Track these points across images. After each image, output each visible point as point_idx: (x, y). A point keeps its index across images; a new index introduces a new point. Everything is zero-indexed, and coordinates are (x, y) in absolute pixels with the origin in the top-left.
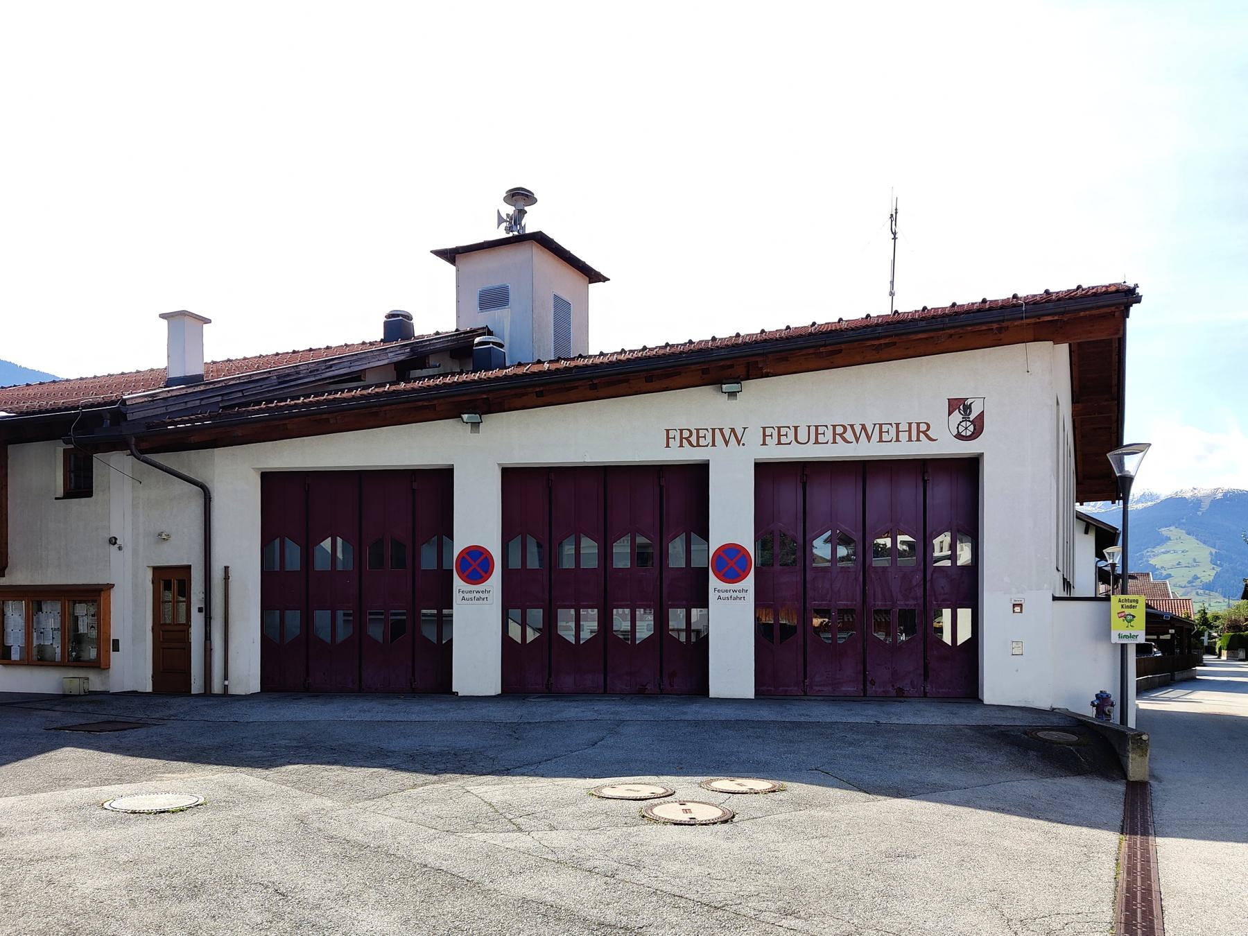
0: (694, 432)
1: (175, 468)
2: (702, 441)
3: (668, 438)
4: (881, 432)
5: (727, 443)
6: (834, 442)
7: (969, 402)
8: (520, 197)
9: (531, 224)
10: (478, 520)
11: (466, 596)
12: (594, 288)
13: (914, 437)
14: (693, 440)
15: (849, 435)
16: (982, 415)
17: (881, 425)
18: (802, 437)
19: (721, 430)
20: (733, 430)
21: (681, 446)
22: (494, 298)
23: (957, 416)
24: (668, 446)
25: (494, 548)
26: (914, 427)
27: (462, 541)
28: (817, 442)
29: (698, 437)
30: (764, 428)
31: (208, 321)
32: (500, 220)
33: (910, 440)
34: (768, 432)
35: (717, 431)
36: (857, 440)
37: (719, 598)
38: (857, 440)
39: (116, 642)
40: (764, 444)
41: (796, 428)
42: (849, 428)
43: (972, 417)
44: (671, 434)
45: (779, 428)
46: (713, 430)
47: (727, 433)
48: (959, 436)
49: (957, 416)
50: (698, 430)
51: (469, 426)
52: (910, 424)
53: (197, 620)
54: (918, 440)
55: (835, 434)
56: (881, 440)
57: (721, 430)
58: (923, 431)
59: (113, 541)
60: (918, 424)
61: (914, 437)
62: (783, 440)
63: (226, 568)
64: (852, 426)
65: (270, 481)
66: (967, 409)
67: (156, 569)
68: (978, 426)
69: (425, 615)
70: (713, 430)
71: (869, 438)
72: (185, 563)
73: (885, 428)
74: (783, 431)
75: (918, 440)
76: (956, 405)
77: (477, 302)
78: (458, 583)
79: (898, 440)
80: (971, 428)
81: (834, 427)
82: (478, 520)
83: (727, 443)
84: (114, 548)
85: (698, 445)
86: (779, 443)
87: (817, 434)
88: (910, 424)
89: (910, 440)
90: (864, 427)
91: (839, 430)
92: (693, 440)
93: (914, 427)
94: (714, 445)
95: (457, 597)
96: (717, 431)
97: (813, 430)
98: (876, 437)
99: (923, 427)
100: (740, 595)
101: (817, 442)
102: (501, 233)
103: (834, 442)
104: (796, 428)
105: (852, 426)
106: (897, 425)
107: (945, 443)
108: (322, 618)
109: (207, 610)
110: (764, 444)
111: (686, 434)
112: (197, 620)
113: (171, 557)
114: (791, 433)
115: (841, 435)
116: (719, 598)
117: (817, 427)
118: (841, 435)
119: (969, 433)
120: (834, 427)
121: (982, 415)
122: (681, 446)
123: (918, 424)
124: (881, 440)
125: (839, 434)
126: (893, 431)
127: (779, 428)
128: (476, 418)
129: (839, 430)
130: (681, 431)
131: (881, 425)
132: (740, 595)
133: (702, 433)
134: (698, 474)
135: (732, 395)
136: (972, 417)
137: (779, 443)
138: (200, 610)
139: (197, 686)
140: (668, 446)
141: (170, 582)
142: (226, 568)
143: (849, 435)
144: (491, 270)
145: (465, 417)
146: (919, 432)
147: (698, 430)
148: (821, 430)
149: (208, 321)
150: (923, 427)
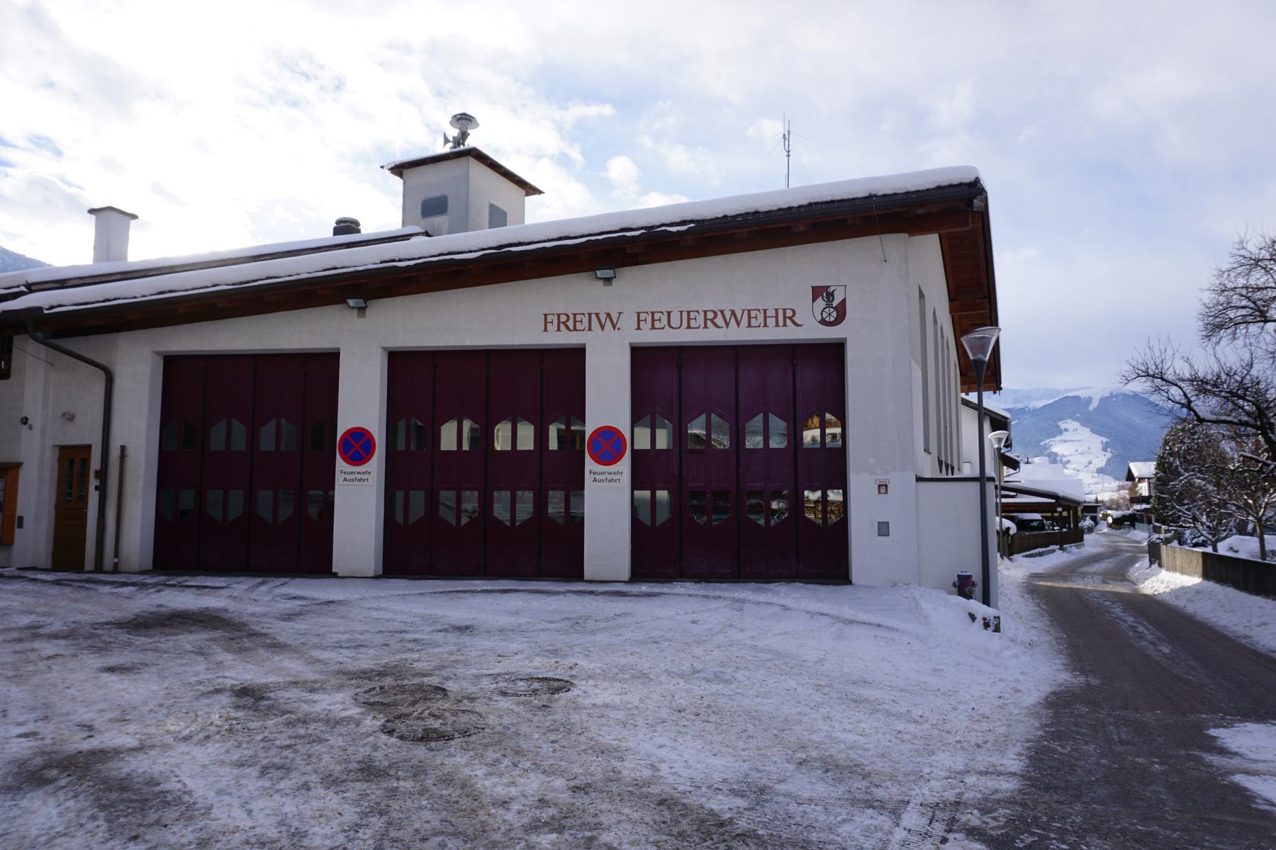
1: (77, 351)
2: (579, 326)
3: (546, 323)
4: (749, 318)
5: (603, 327)
6: (706, 327)
7: (831, 289)
8: (464, 120)
9: (470, 143)
10: (361, 402)
11: (349, 477)
12: (531, 200)
13: (781, 323)
14: (571, 324)
15: (719, 321)
16: (843, 302)
17: (749, 311)
18: (675, 321)
19: (597, 315)
20: (608, 315)
21: (559, 330)
22: (433, 207)
23: (821, 303)
24: (546, 330)
25: (377, 429)
26: (781, 312)
27: (346, 421)
28: (689, 327)
29: (575, 322)
30: (639, 314)
31: (134, 217)
32: (446, 141)
33: (777, 325)
34: (642, 317)
35: (594, 317)
36: (727, 324)
37: (595, 480)
38: (727, 324)
39: (21, 518)
40: (639, 328)
41: (669, 313)
43: (835, 304)
44: (549, 318)
45: (653, 313)
46: (590, 315)
47: (603, 317)
48: (823, 322)
49: (821, 303)
50: (575, 315)
51: (355, 312)
52: (777, 310)
53: (93, 497)
54: (785, 325)
55: (706, 319)
57: (597, 315)
58: (789, 317)
59: (25, 421)
60: (784, 310)
61: (781, 323)
62: (657, 324)
63: (123, 448)
64: (722, 312)
65: (174, 366)
66: (830, 296)
68: (841, 311)
70: (590, 315)
71: (738, 323)
72: (86, 442)
73: (753, 314)
74: (657, 316)
75: (785, 325)
76: (818, 292)
77: (419, 210)
79: (765, 325)
80: (835, 314)
81: (705, 312)
82: (361, 402)
83: (603, 327)
84: (25, 428)
85: (575, 329)
86: (653, 328)
87: (689, 319)
88: (777, 310)
89: (777, 325)
90: (733, 313)
91: (710, 315)
92: (571, 324)
93: (781, 312)
94: (590, 329)
95: (339, 478)
96: (594, 317)
97: (685, 315)
98: (745, 322)
99: (789, 313)
100: (615, 477)
101: (689, 327)
102: (447, 149)
103: (706, 327)
104: (669, 313)
105: (722, 312)
106: (765, 311)
107: (810, 329)
109: (102, 490)
110: (639, 328)
111: (563, 318)
112: (93, 497)
113: (74, 436)
114: (664, 318)
115: (712, 320)
116: (595, 480)
117: (689, 313)
118: (712, 320)
121: (843, 302)
122: (559, 330)
123: (784, 310)
124: (749, 325)
125: (710, 319)
126: (761, 317)
127: (653, 313)
128: (361, 303)
129: (710, 315)
130: (559, 315)
131: (749, 311)
132: (615, 477)
133: (578, 318)
134: (576, 355)
135: (608, 281)
136: (835, 304)
137: (653, 328)
139: (89, 562)
140: (546, 330)
141: (72, 462)
142: (123, 448)
144: (431, 180)
145: (351, 302)
146: (785, 318)
147: (575, 315)
150: (789, 313)
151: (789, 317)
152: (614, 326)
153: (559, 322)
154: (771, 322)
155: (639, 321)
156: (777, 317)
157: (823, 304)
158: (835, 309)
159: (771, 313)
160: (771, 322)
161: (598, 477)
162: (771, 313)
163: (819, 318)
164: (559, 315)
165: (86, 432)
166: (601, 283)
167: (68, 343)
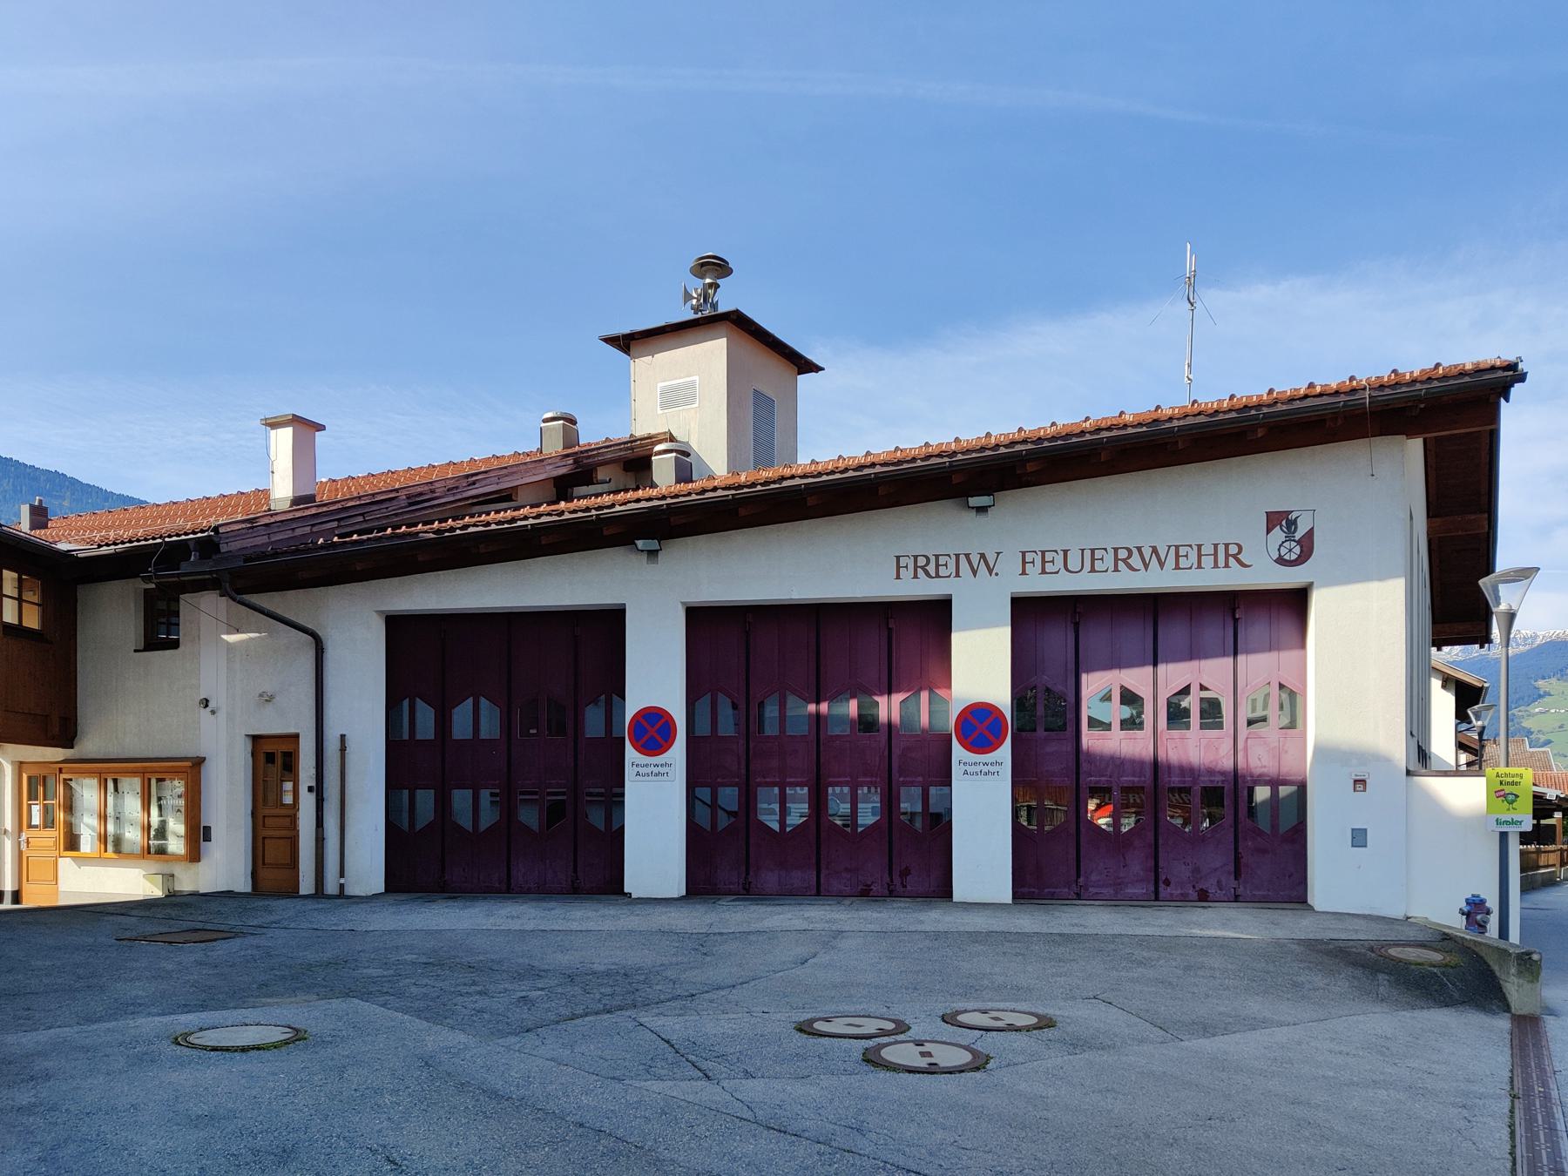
0: (933, 559)
1: (279, 612)
3: (898, 567)
4: (1177, 556)
5: (975, 573)
6: (1116, 570)
7: (1293, 516)
8: (715, 267)
10: (656, 675)
12: (804, 380)
13: (1221, 562)
14: (931, 569)
15: (1135, 561)
16: (1310, 533)
17: (1177, 547)
18: (1074, 563)
19: (967, 556)
20: (983, 556)
21: (916, 577)
23: (1278, 534)
24: (898, 577)
25: (677, 709)
26: (1221, 549)
27: (635, 701)
28: (1093, 570)
29: (937, 566)
30: (1024, 554)
31: (321, 428)
32: (687, 296)
33: (1216, 566)
35: (962, 558)
36: (1146, 566)
37: (966, 773)
38: (1146, 566)
39: (207, 830)
41: (1065, 552)
42: (1135, 551)
44: (903, 562)
45: (1043, 553)
46: (957, 556)
47: (975, 559)
48: (1281, 561)
49: (1278, 534)
50: (937, 557)
51: (645, 556)
52: (1216, 546)
53: (307, 802)
54: (1227, 566)
55: (1116, 559)
56: (1177, 567)
59: (206, 703)
60: (1227, 546)
61: (1221, 562)
63: (343, 737)
64: (1139, 549)
65: (399, 627)
66: (1292, 525)
67: (256, 739)
68: (1307, 547)
69: (590, 794)
70: (957, 556)
71: (1162, 564)
72: (292, 730)
73: (1182, 551)
74: (1048, 557)
75: (1227, 566)
76: (1275, 519)
78: (631, 753)
79: (1199, 566)
80: (1297, 550)
81: (1116, 550)
82: (656, 675)
83: (975, 573)
84: (205, 713)
85: (938, 576)
86: (1044, 572)
87: (1093, 559)
88: (1216, 546)
89: (1216, 566)
90: (1155, 550)
91: (1123, 554)
92: (931, 569)
93: (1221, 549)
94: (957, 575)
95: (629, 772)
96: (962, 558)
97: (1088, 554)
98: (1171, 563)
99: (1233, 550)
100: (992, 769)
101: (1093, 570)
103: (1116, 570)
104: (1065, 552)
105: (1139, 549)
106: (1199, 547)
108: (461, 799)
109: (318, 790)
110: (1024, 573)
113: (272, 725)
114: (1059, 559)
115: (1124, 561)
116: (966, 773)
117: (1093, 551)
118: (1124, 561)
119: (1294, 557)
120: (1116, 550)
121: (1310, 533)
122: (916, 577)
123: (1227, 546)
124: (1177, 567)
126: (1193, 555)
127: (1043, 553)
128: (653, 544)
129: (1123, 554)
131: (1177, 547)
132: (992, 769)
133: (942, 560)
135: (982, 510)
136: (1298, 536)
137: (1044, 572)
138: (310, 789)
139: (306, 885)
140: (898, 577)
141: (272, 758)
142: (343, 737)
143: (1135, 561)
145: (640, 543)
146: (1227, 555)
147: (937, 557)
148: (1098, 554)
149: (321, 428)
150: (1233, 550)
151: (1233, 555)
152: (990, 571)
153: (916, 567)
154: (1208, 561)
155: (1024, 563)
156: (1216, 554)
157: (1282, 536)
158: (1298, 542)
159: (1208, 549)
160: (1208, 561)
161: (970, 769)
162: (1208, 549)
163: (1276, 556)
164: (916, 557)
165: (293, 718)
166: (974, 513)
167: (254, 599)
